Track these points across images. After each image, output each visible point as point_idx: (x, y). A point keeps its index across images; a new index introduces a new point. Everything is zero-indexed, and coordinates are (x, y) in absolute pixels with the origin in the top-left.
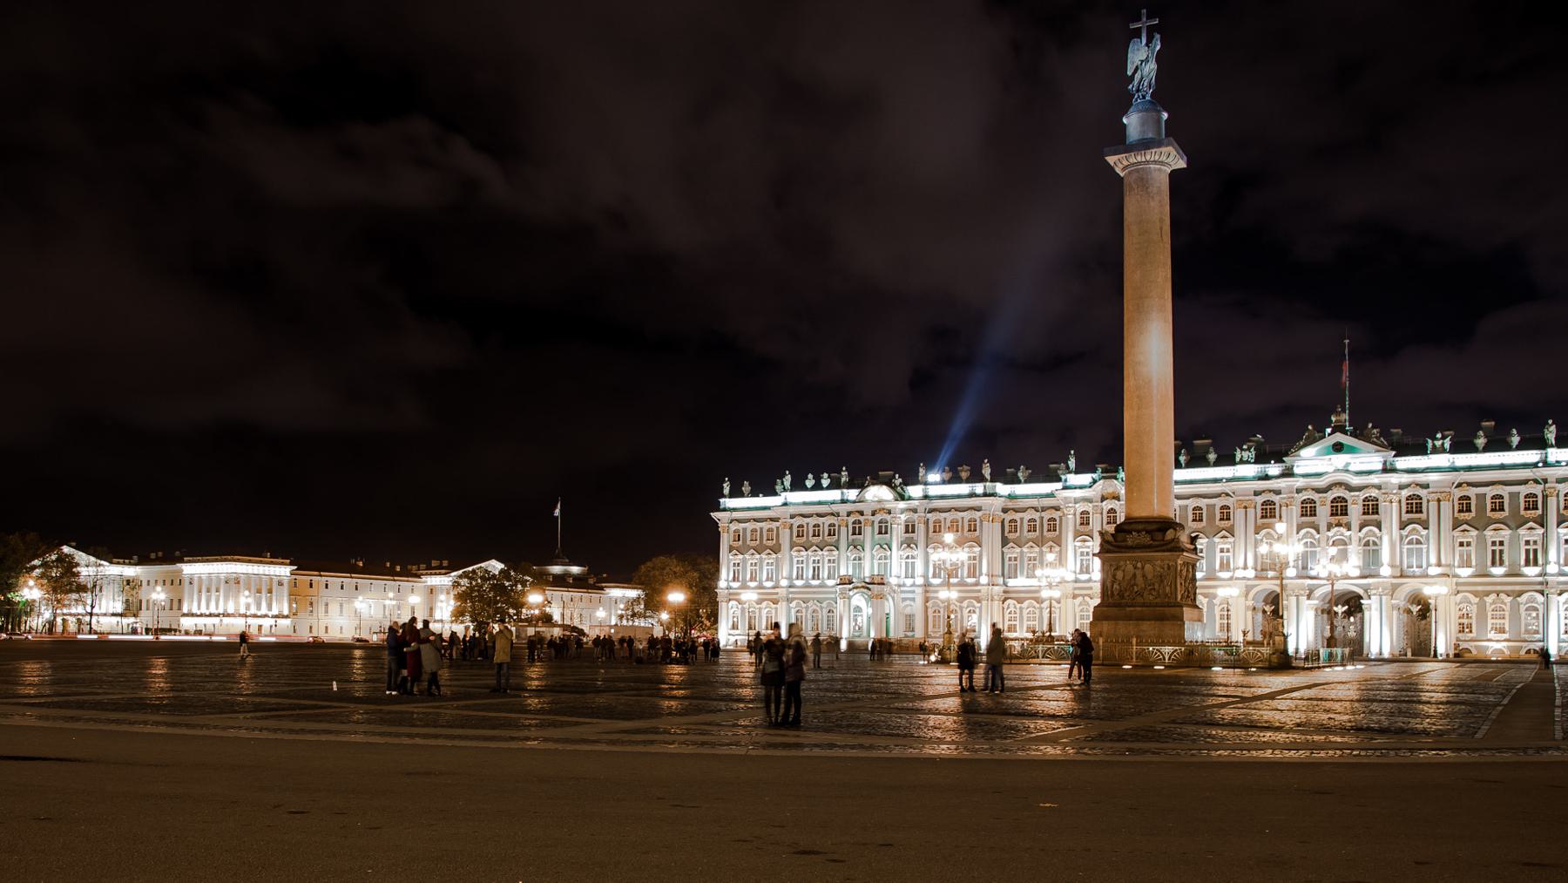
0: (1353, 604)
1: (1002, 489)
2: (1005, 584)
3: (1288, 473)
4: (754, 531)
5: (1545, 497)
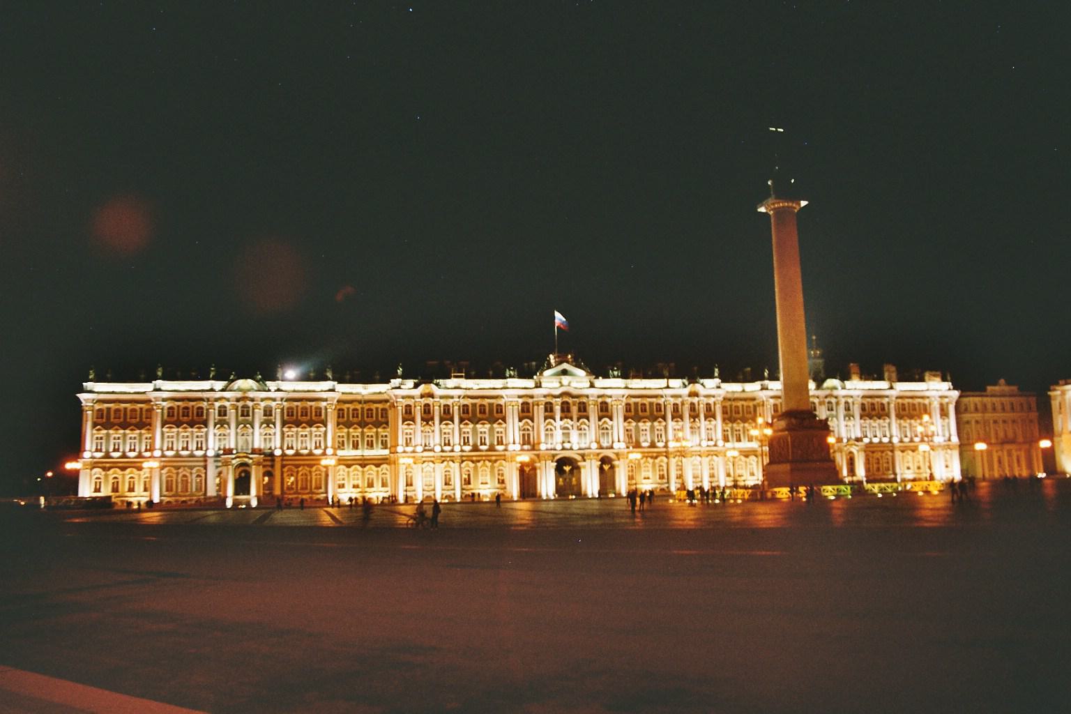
3: (538, 386)
4: (117, 411)
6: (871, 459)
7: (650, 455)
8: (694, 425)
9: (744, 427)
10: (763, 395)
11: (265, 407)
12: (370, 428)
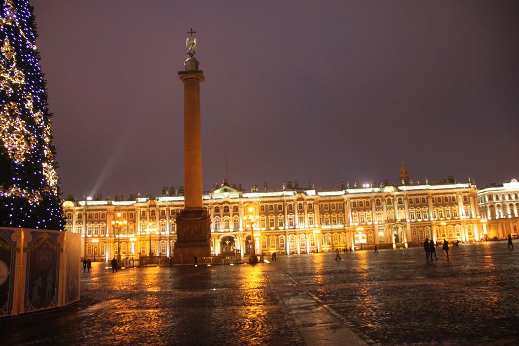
0: (231, 239)
1: (114, 203)
2: (115, 237)
5: (284, 206)
6: (417, 231)
7: (275, 234)
8: (301, 216)
10: (345, 197)
11: (79, 214)
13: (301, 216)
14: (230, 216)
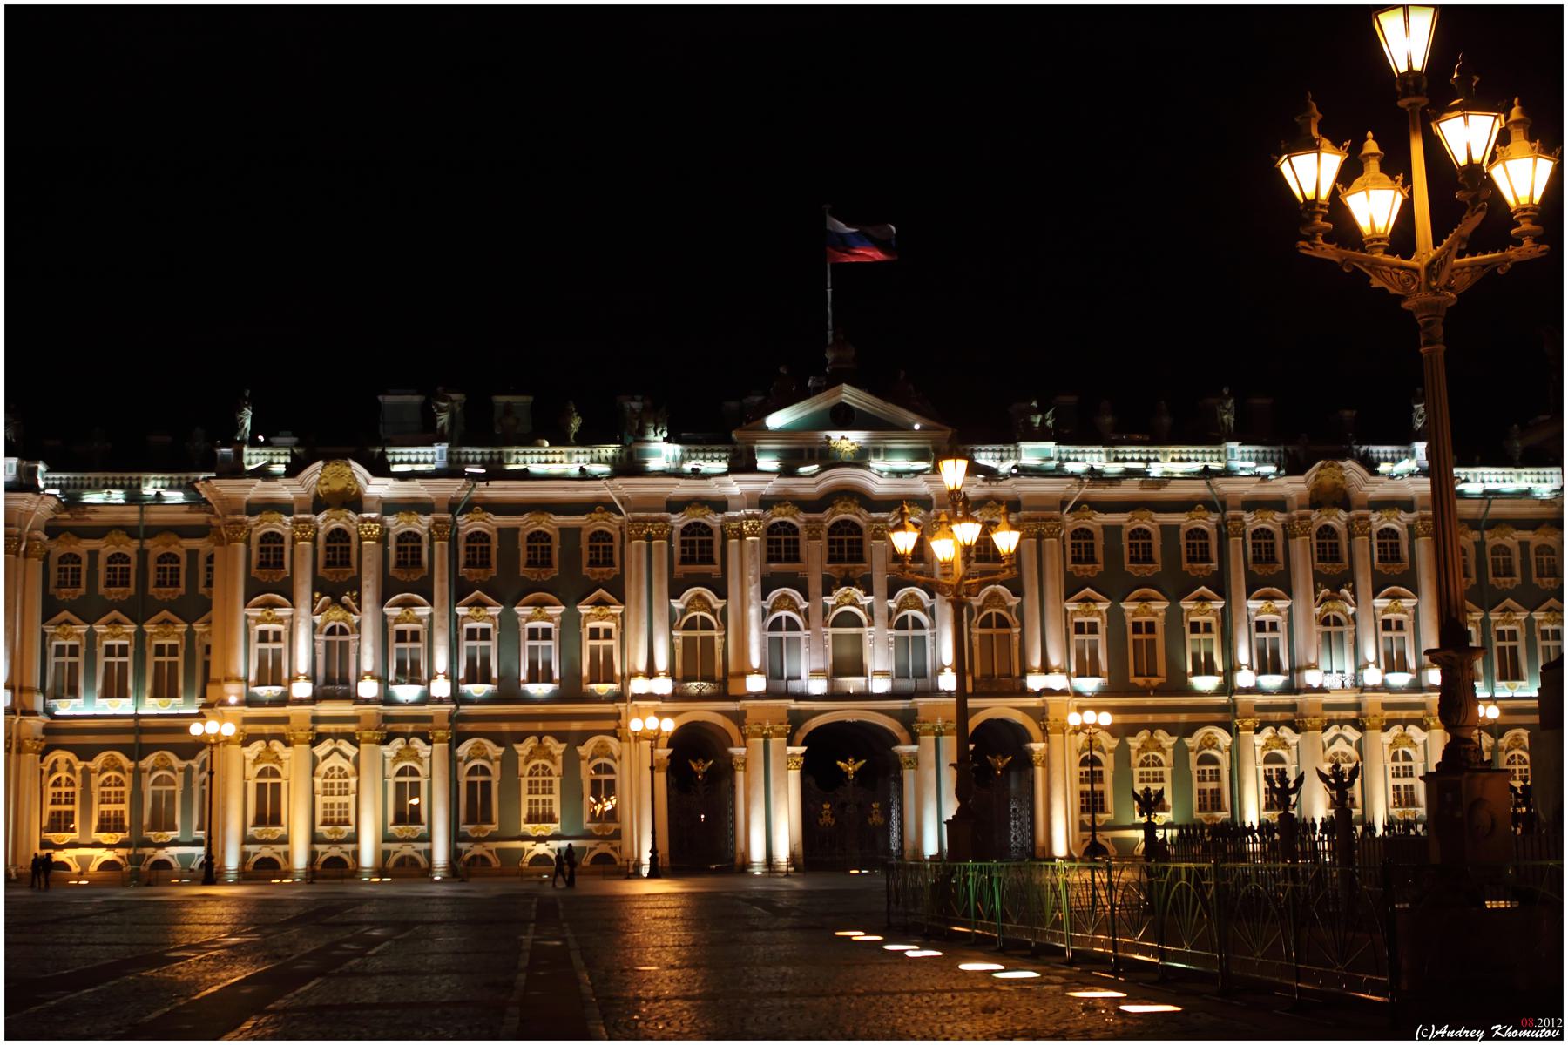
2: (49, 712)
5: (1223, 538)
7: (1168, 718)
8: (1334, 609)
9: (1530, 622)
12: (166, 622)
13: (1334, 609)
14: (869, 593)
